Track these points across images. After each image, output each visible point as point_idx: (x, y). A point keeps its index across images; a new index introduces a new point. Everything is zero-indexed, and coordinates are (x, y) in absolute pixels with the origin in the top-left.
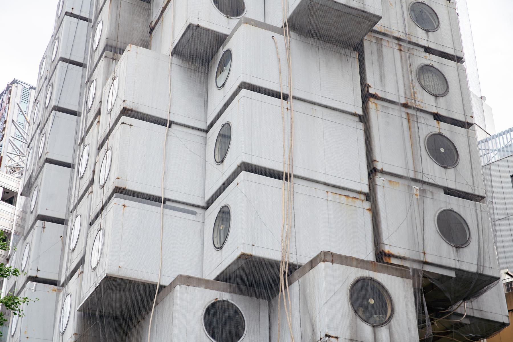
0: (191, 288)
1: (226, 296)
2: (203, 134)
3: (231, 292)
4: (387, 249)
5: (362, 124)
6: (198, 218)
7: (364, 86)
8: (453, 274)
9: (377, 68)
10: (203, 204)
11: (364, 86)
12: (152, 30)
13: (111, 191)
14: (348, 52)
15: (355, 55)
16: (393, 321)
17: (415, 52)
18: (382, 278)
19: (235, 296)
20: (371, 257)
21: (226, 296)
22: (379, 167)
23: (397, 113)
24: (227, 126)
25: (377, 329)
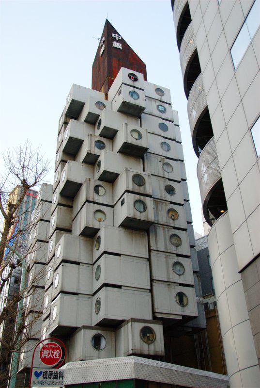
0: (87, 330)
1: (99, 332)
2: (92, 266)
3: (101, 330)
4: (157, 311)
5: (148, 262)
6: (90, 299)
7: (149, 246)
8: (181, 318)
9: (154, 240)
10: (92, 294)
11: (149, 246)
12: (73, 220)
13: (58, 292)
14: (143, 233)
15: (146, 234)
16: (155, 342)
17: (169, 230)
18: (153, 326)
19: (103, 331)
20: (150, 318)
21: (99, 332)
22: (155, 278)
23: (163, 255)
24: (99, 266)
25: (150, 345)
